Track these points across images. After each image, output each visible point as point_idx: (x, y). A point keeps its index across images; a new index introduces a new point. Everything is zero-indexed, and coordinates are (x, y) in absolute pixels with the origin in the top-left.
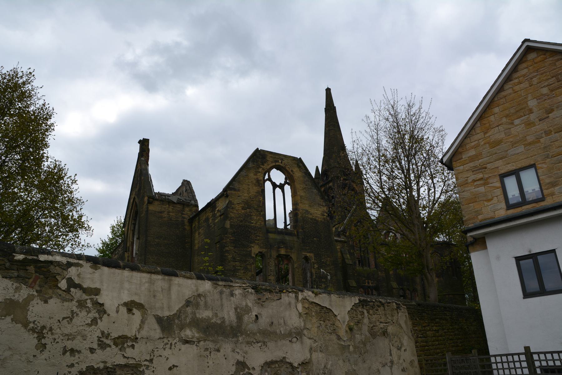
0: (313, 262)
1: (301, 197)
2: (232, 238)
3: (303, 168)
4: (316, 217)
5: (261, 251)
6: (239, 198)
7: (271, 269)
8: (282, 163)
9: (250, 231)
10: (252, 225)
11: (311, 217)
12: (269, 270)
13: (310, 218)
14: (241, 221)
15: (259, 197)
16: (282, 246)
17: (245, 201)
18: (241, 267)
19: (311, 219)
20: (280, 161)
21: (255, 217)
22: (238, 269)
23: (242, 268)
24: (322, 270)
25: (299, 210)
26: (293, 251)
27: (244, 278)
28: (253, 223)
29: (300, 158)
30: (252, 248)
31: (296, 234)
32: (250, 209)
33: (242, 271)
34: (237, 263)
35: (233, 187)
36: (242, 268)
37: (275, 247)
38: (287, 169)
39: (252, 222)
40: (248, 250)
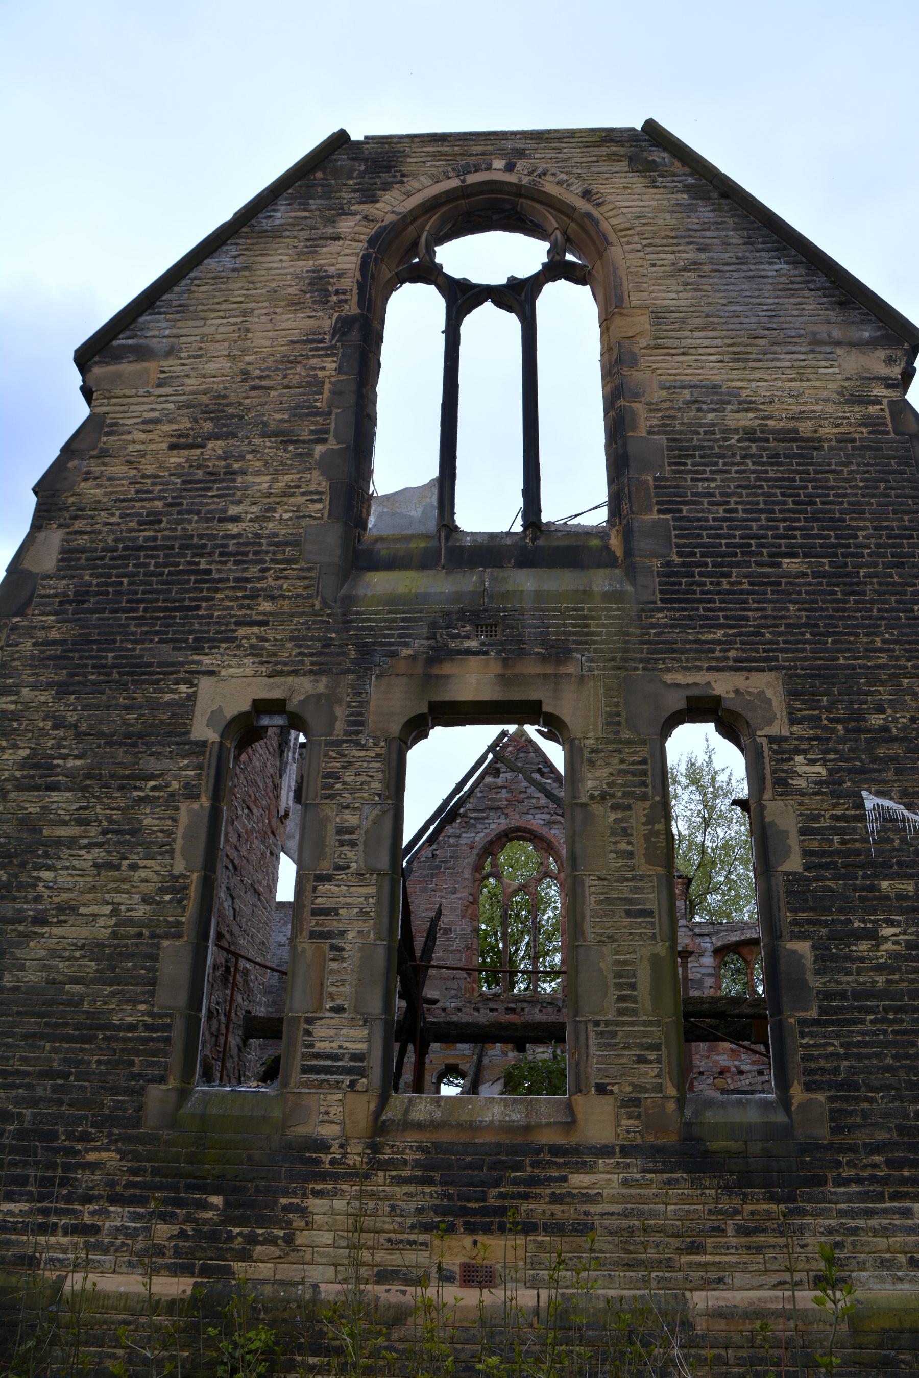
0: (772, 740)
1: (659, 316)
2: (54, 635)
3: (677, 166)
4: (800, 417)
5: (276, 694)
6: (162, 391)
7: (351, 819)
8: (510, 168)
9: (208, 572)
10: (233, 528)
11: (747, 420)
12: (331, 838)
13: (736, 431)
14: (153, 520)
15: (314, 362)
16: (474, 644)
17: (205, 399)
18: (80, 822)
19: (750, 435)
20: (499, 164)
21: (263, 482)
22: (58, 842)
23: (94, 831)
24: (870, 801)
25: (636, 396)
26: (570, 669)
27: (94, 909)
28: (236, 519)
29: (650, 125)
30: (205, 683)
31: (619, 553)
32: (234, 435)
33: (87, 858)
34: (55, 796)
35: (130, 342)
36: (94, 830)
37: (406, 652)
38: (551, 188)
39: (233, 510)
40: (168, 697)
